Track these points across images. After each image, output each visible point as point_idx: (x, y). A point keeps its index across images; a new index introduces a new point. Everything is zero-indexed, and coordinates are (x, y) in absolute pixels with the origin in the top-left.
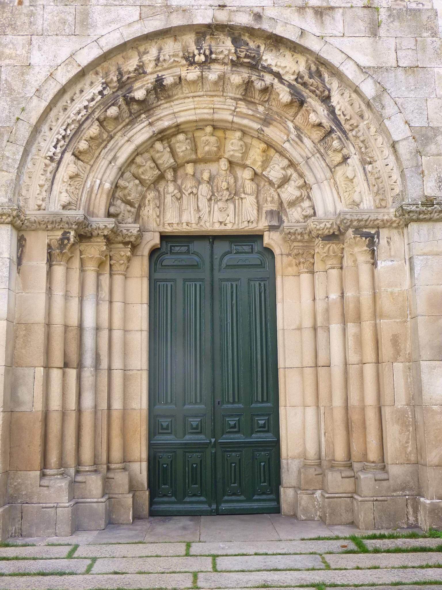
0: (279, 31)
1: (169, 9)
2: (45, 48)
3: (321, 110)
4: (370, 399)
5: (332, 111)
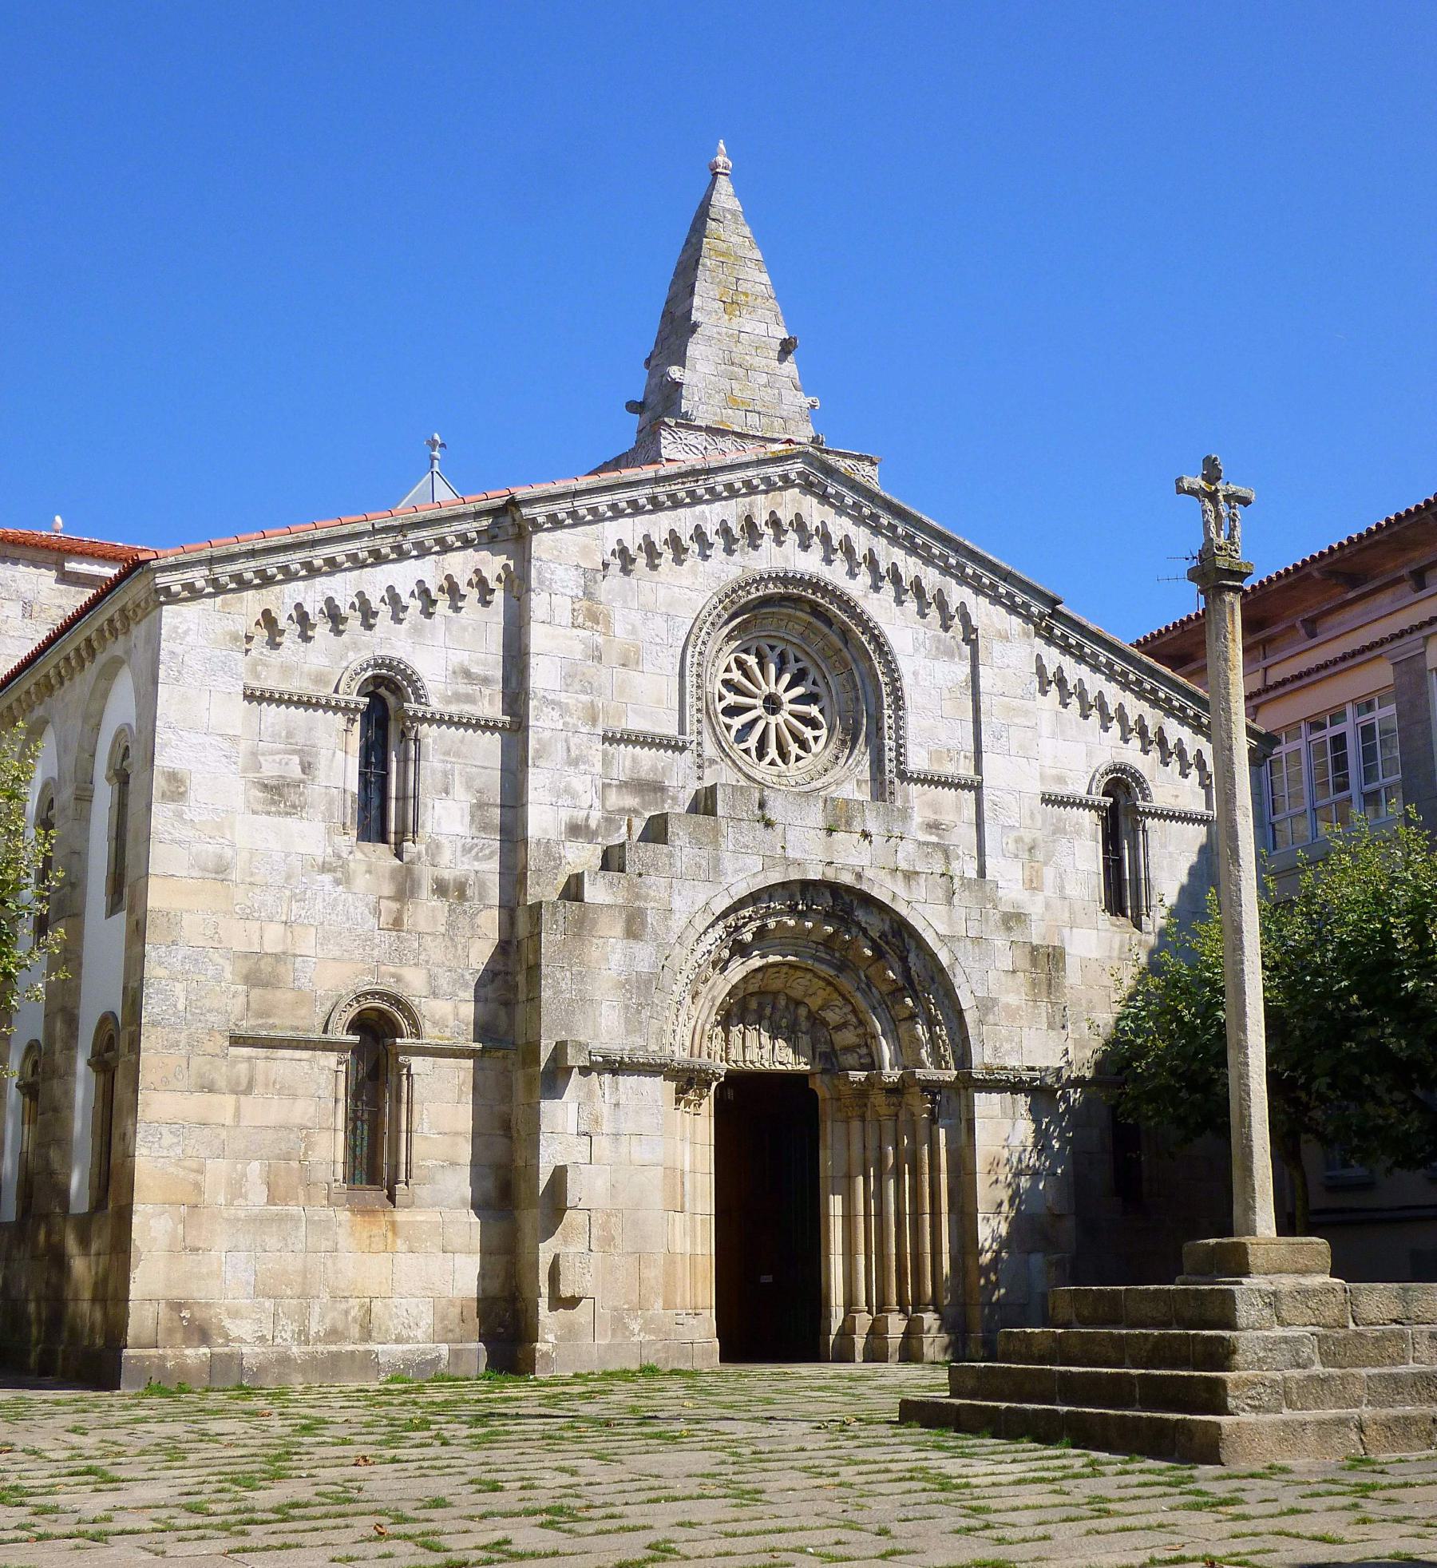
0: (875, 893)
1: (788, 862)
2: (684, 893)
3: (897, 965)
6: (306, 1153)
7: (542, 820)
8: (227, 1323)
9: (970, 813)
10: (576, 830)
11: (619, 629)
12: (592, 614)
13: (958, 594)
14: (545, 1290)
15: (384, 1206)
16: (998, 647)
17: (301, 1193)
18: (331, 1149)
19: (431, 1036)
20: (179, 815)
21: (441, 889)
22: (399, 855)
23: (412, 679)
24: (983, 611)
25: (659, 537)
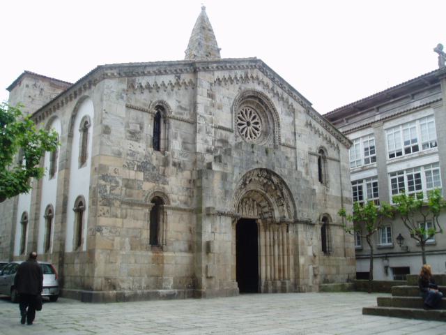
4: (286, 263)
5: (282, 193)
7: (200, 147)
8: (121, 284)
9: (293, 155)
10: (208, 151)
11: (218, 100)
12: (211, 96)
13: (291, 100)
14: (204, 275)
16: (299, 114)
18: (146, 234)
19: (173, 204)
20: (109, 138)
21: (174, 164)
22: (164, 154)
23: (168, 106)
24: (297, 106)
25: (227, 77)
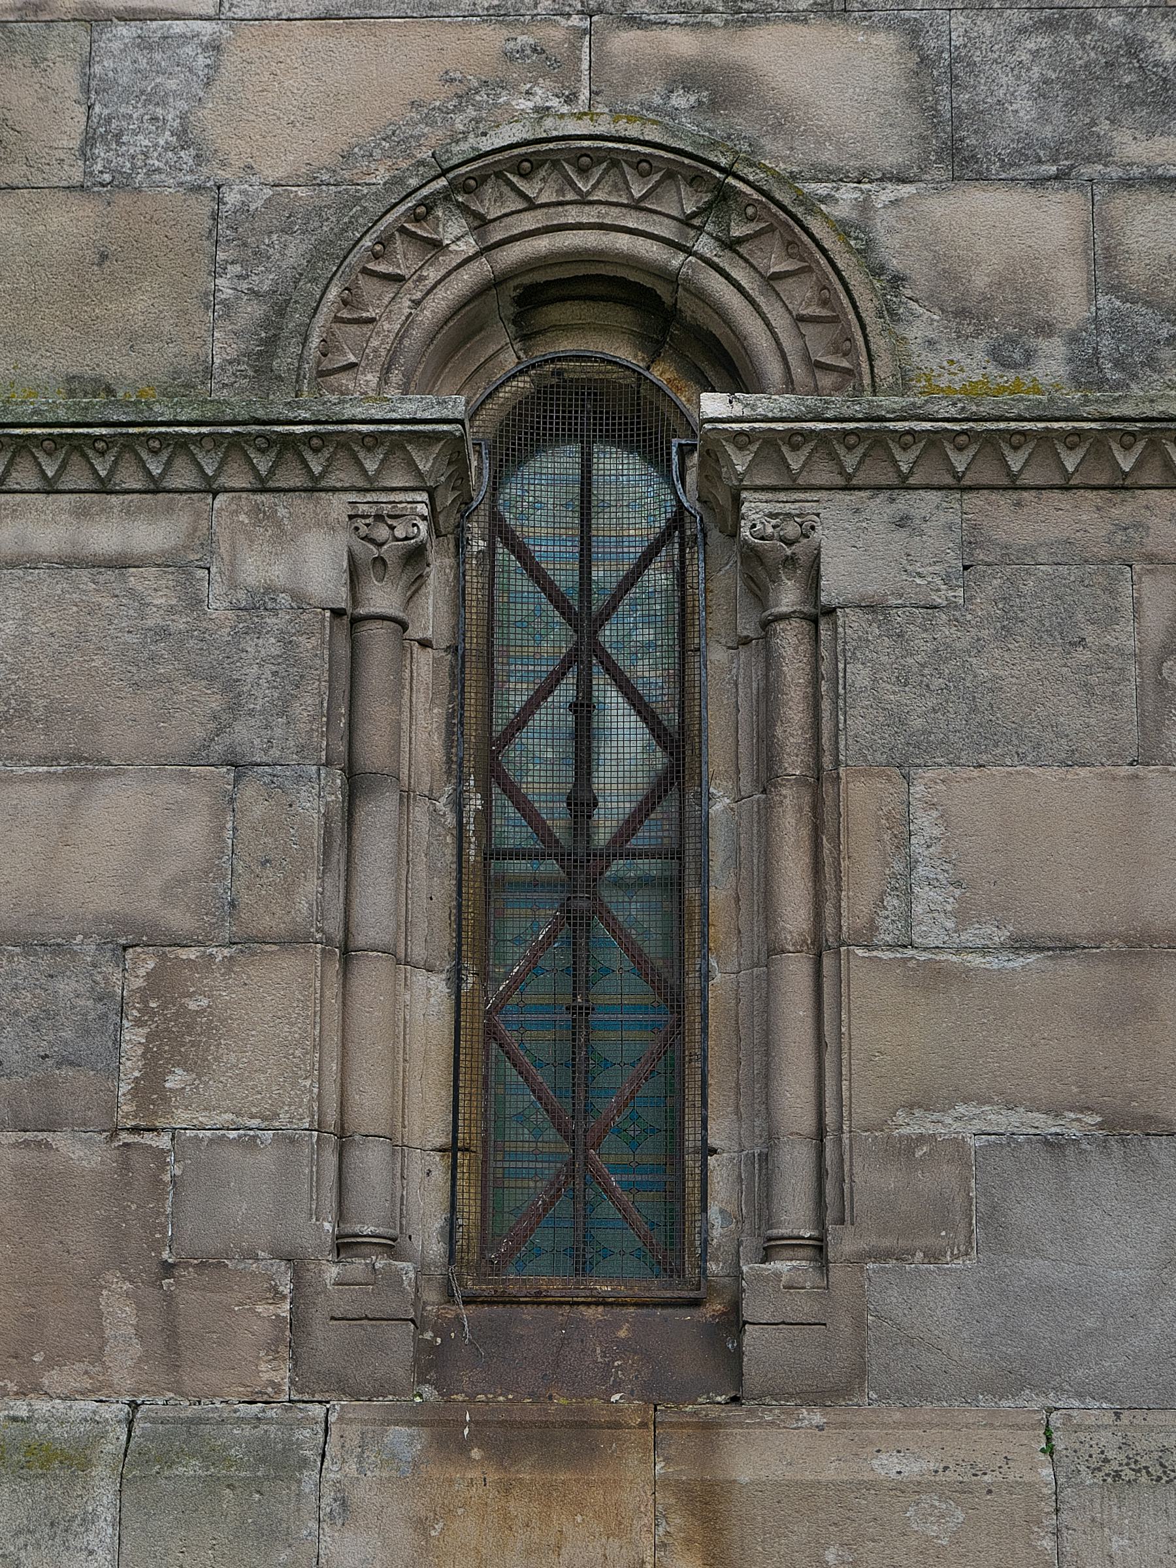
6: (150, 1092)
15: (658, 1392)
17: (120, 1311)
18: (344, 1070)
